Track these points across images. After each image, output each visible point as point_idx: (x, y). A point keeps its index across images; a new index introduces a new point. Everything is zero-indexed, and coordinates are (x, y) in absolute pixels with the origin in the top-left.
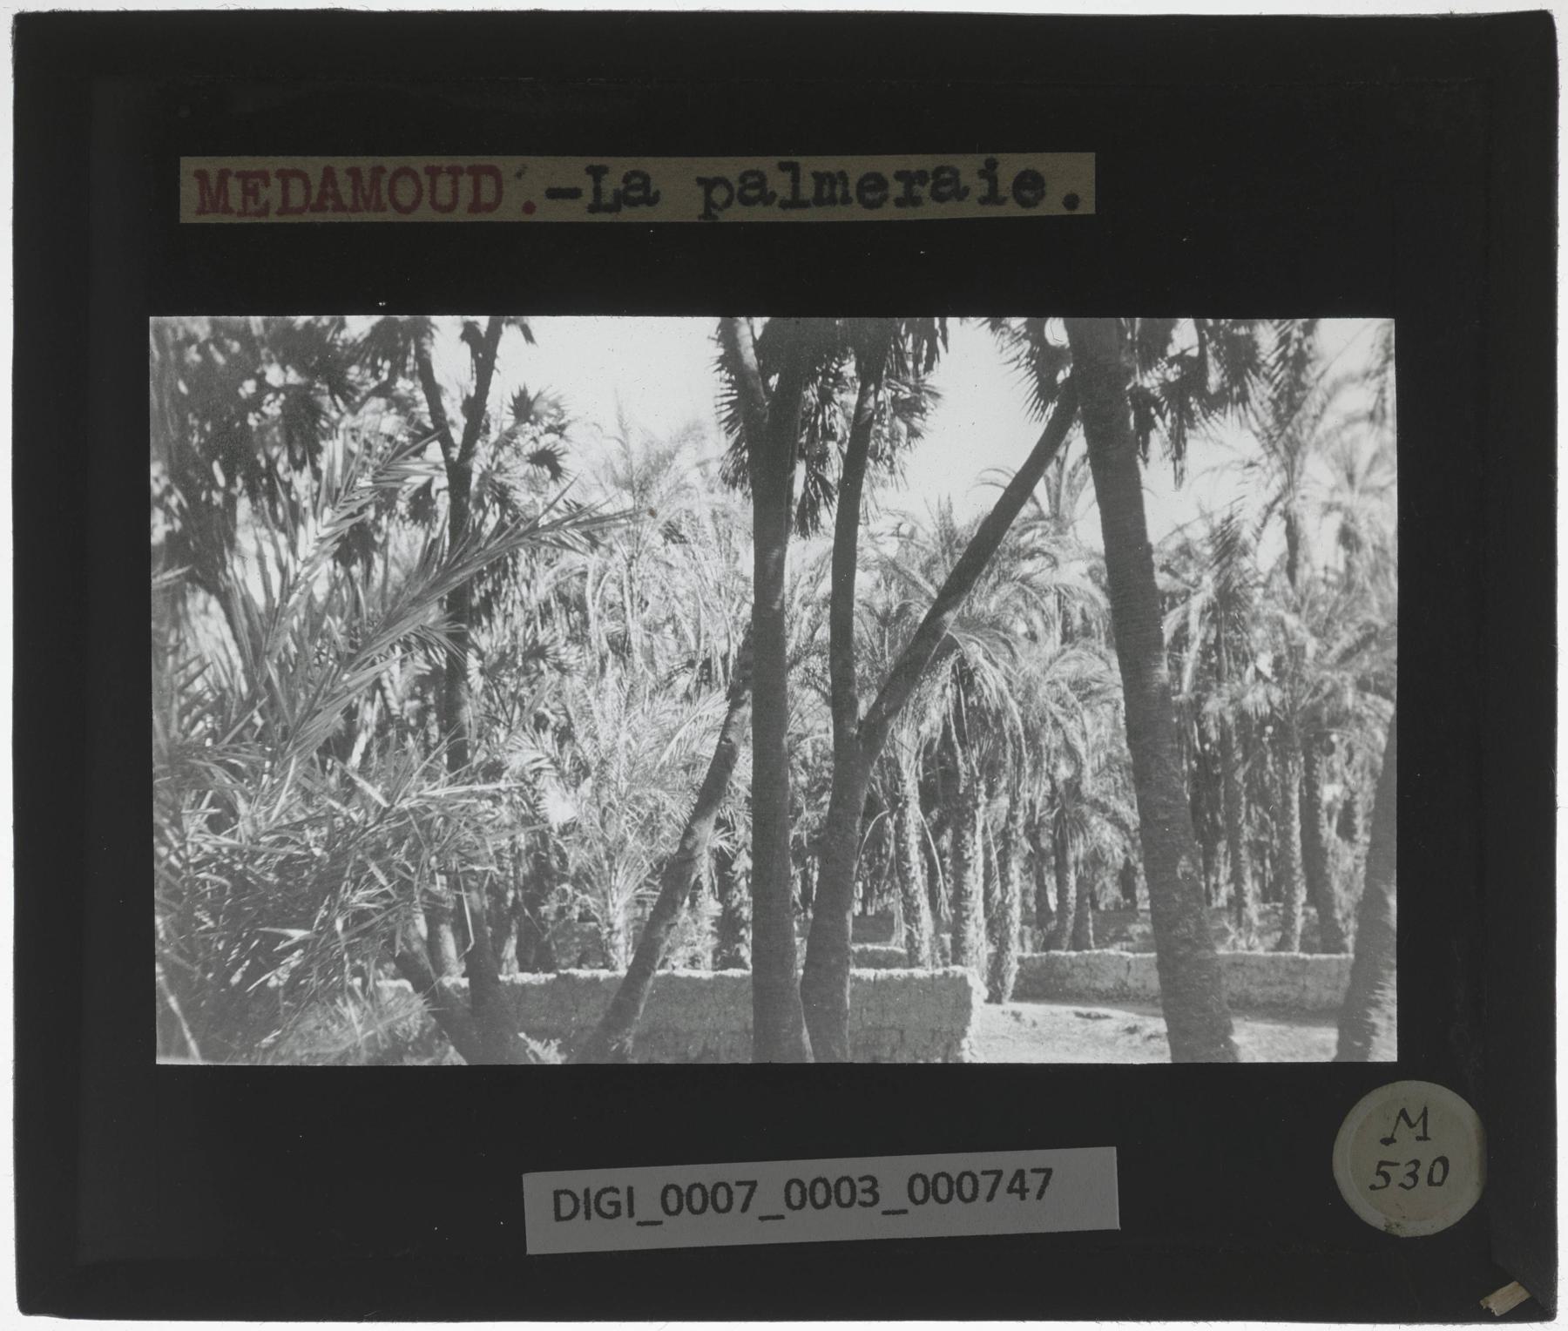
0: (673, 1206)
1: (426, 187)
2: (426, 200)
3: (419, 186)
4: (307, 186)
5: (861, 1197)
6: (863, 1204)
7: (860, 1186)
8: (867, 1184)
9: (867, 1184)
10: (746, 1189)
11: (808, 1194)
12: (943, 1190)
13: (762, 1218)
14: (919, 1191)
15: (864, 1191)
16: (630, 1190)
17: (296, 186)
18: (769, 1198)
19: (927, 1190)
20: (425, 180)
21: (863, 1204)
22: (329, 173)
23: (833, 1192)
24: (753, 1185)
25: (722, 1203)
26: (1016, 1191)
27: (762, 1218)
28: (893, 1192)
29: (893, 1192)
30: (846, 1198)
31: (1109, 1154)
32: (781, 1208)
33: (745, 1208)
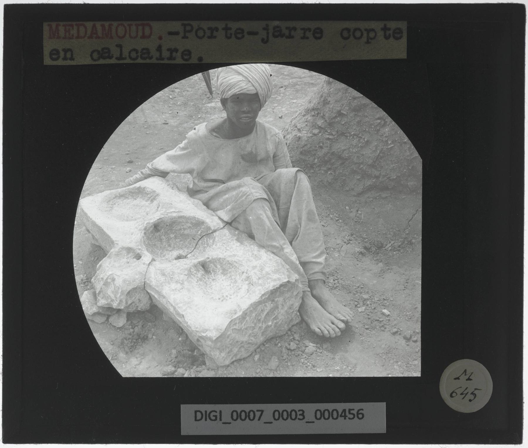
0: (235, 417)
1: (128, 31)
2: (127, 35)
3: (125, 29)
4: (86, 32)
5: (299, 417)
6: (299, 419)
7: (298, 413)
8: (301, 412)
9: (301, 412)
10: (260, 413)
11: (281, 415)
12: (326, 416)
13: (265, 423)
14: (318, 416)
15: (300, 415)
16: (221, 412)
17: (82, 29)
18: (268, 416)
19: (321, 415)
20: (128, 28)
21: (299, 419)
22: (94, 26)
23: (289, 415)
24: (262, 411)
25: (252, 417)
26: (342, 416)
27: (265, 423)
28: (310, 415)
29: (310, 415)
30: (293, 417)
31: (384, 404)
32: (272, 420)
33: (259, 420)
